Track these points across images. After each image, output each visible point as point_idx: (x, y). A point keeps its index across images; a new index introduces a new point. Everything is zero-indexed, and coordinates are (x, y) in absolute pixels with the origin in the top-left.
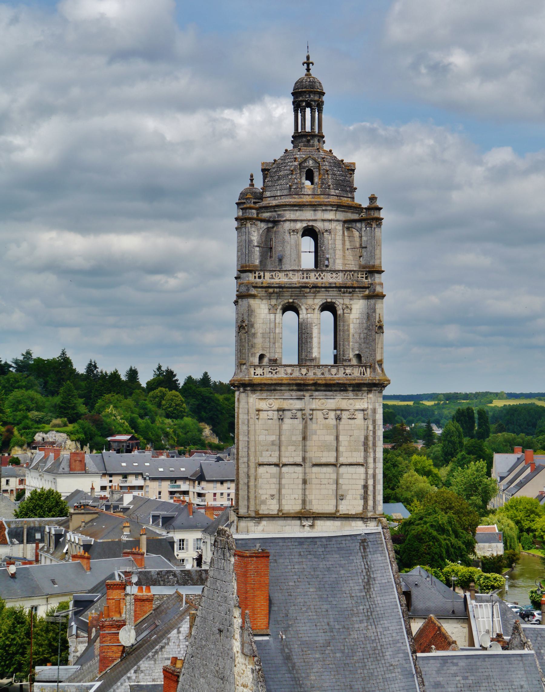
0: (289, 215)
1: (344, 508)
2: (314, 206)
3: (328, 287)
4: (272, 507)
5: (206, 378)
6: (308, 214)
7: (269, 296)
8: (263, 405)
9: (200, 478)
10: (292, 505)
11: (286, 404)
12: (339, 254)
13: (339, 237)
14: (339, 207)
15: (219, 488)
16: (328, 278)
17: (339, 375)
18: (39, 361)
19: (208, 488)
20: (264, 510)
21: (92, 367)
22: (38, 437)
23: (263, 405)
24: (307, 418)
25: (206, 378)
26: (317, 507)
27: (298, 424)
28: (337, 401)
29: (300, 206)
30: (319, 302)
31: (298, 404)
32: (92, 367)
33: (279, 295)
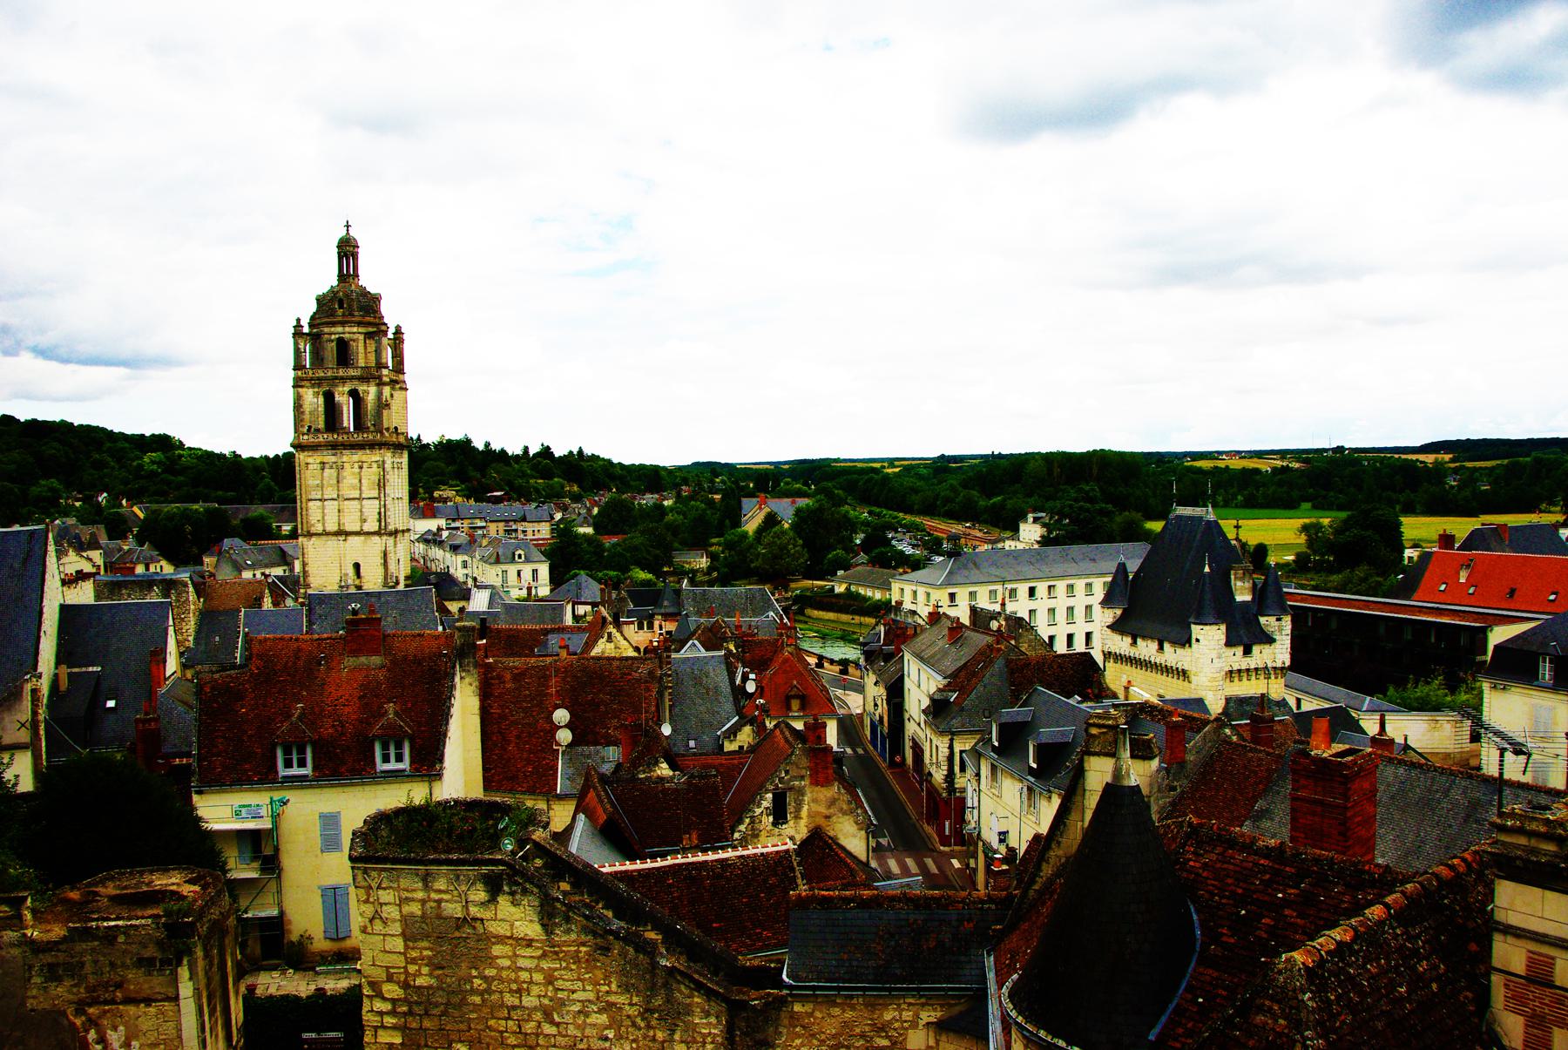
0: (326, 330)
1: (366, 528)
2: (343, 324)
3: (352, 378)
4: (319, 528)
5: (580, 451)
6: (340, 329)
7: (313, 386)
8: (310, 460)
9: (524, 519)
10: (332, 526)
11: (326, 459)
12: (361, 356)
13: (361, 344)
14: (359, 324)
15: (536, 527)
16: (352, 372)
17: (359, 438)
18: (449, 441)
19: (529, 527)
20: (313, 530)
21: (487, 445)
22: (436, 494)
23: (310, 460)
24: (340, 468)
25: (580, 451)
26: (348, 528)
27: (334, 472)
28: (359, 456)
29: (334, 324)
30: (346, 389)
31: (333, 459)
32: (487, 445)
33: (319, 385)
